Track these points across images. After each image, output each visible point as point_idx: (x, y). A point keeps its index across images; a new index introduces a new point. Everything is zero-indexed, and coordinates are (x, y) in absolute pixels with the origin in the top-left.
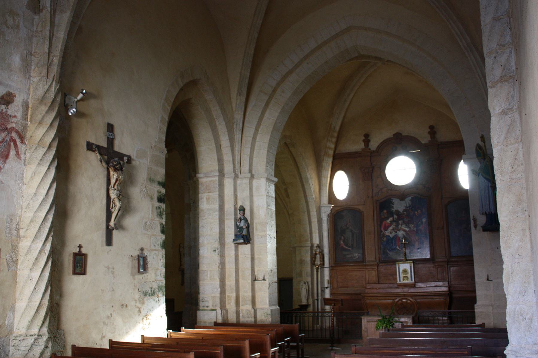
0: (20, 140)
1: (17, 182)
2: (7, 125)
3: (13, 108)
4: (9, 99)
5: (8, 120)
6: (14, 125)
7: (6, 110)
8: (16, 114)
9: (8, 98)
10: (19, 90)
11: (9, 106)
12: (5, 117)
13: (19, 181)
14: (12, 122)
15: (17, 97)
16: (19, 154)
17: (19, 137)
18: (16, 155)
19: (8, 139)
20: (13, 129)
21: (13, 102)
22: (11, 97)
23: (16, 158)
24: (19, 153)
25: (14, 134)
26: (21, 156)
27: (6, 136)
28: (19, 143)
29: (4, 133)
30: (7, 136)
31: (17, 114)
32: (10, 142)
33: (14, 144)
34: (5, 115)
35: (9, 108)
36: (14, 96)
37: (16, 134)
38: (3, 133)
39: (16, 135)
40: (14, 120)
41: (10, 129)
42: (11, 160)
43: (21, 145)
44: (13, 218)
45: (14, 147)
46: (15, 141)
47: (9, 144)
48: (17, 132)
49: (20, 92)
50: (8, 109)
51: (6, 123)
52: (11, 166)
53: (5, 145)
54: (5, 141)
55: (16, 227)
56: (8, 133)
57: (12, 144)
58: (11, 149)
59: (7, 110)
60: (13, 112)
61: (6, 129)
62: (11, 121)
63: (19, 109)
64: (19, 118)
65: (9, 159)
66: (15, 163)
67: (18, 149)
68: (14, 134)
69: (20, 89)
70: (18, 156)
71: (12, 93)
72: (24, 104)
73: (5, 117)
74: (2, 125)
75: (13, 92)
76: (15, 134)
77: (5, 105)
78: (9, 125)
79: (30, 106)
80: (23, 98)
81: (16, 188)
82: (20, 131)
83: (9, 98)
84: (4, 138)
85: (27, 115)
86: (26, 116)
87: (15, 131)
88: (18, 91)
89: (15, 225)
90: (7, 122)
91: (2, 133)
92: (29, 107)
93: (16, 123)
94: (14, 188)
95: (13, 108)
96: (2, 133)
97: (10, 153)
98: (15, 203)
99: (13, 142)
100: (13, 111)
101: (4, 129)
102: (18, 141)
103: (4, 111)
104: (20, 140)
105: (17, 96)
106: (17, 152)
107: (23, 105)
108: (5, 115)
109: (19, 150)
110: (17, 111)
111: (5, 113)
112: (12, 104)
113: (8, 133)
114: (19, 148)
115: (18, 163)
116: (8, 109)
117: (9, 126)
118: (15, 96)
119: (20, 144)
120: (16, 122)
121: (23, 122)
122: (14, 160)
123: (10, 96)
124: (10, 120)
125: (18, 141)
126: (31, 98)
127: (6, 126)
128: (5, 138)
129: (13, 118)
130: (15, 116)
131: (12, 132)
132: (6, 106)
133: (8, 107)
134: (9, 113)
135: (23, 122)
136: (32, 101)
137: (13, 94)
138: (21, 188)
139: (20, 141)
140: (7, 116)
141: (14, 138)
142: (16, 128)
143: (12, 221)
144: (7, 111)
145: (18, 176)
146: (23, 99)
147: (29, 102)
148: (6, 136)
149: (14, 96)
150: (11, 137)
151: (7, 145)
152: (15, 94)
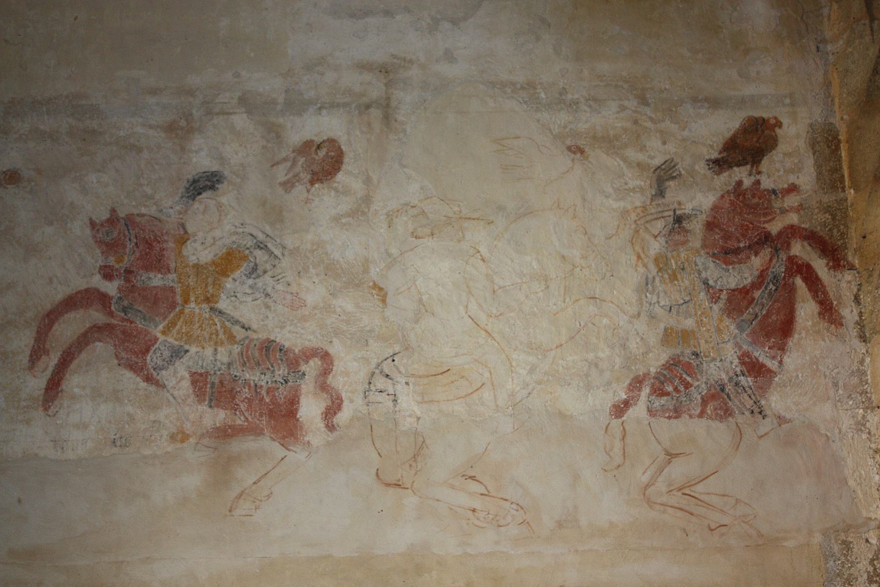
0: (825, 261)
1: (845, 407)
2: (766, 225)
3: (778, 165)
4: (757, 142)
5: (766, 208)
6: (793, 218)
7: (753, 179)
8: (792, 179)
9: (755, 140)
10: (788, 101)
11: (763, 162)
12: (756, 200)
13: (851, 403)
14: (784, 211)
15: (785, 125)
16: (831, 308)
17: (819, 252)
18: (820, 314)
19: (779, 268)
20: (792, 232)
21: (777, 145)
22: (763, 131)
23: (824, 325)
24: (832, 304)
25: (798, 249)
26: (843, 314)
27: (771, 260)
28: (826, 269)
29: (761, 254)
30: (774, 261)
31: (798, 178)
32: (790, 277)
33: (805, 280)
34: (754, 196)
35: (764, 170)
36: (775, 125)
37: (806, 244)
38: (756, 256)
39: (809, 248)
40: (792, 200)
41: (780, 234)
42: (803, 335)
43: (835, 277)
44: (850, 539)
45: (810, 290)
46: (809, 267)
47: (785, 284)
48: (812, 238)
49: (792, 105)
50: (759, 173)
51: (760, 222)
52: (808, 358)
53: (770, 293)
54: (771, 276)
55: (871, 569)
56: (777, 251)
57: (799, 281)
58: (799, 299)
59: (758, 177)
60: (779, 177)
61: (766, 238)
62: (780, 209)
63: (799, 162)
64: (808, 187)
65: (796, 336)
66: (822, 343)
67: (825, 293)
68: (798, 249)
69: (791, 95)
70: (831, 315)
71: (764, 119)
72: (819, 139)
73: (756, 200)
74: (746, 230)
75: (765, 116)
76: (803, 246)
77: (747, 163)
78: (771, 223)
79: (842, 137)
80: (808, 121)
81: (844, 430)
82: (823, 233)
83: (759, 138)
84: (762, 271)
85: (838, 169)
86: (836, 176)
87: (800, 238)
88: (784, 105)
89: (866, 562)
90: (765, 215)
91: (753, 257)
92: (839, 141)
93: (800, 208)
94: (837, 431)
95: (778, 165)
96: (753, 257)
97: (798, 313)
98: (851, 483)
99: (801, 274)
100: (781, 173)
101: (757, 243)
102: (820, 266)
103: (747, 182)
104: (825, 261)
105: (785, 121)
106: (821, 303)
107: (813, 144)
108: (754, 196)
109: (831, 295)
110: (797, 169)
111: (751, 190)
112: (774, 152)
113: (777, 251)
114: (828, 289)
115: (834, 338)
116: (759, 173)
117: (775, 228)
118: (779, 124)
119: (832, 272)
120: (801, 205)
121: (827, 199)
122: (818, 332)
123: (760, 132)
124: (777, 204)
125: (820, 266)
126: (840, 107)
127: (764, 228)
128: (767, 269)
129: (783, 196)
130: (793, 189)
131: (789, 245)
132: (752, 166)
133: (757, 167)
134: (767, 183)
135: (827, 199)
136: (845, 117)
137: (769, 119)
138: (864, 425)
139: (828, 264)
140: (760, 198)
141: (801, 259)
142: (803, 226)
143: (849, 549)
144: (758, 182)
145: (841, 384)
146: (811, 125)
147: (837, 125)
148: (771, 260)
149: (775, 125)
150: (791, 259)
151: (780, 289)
152: (776, 118)
